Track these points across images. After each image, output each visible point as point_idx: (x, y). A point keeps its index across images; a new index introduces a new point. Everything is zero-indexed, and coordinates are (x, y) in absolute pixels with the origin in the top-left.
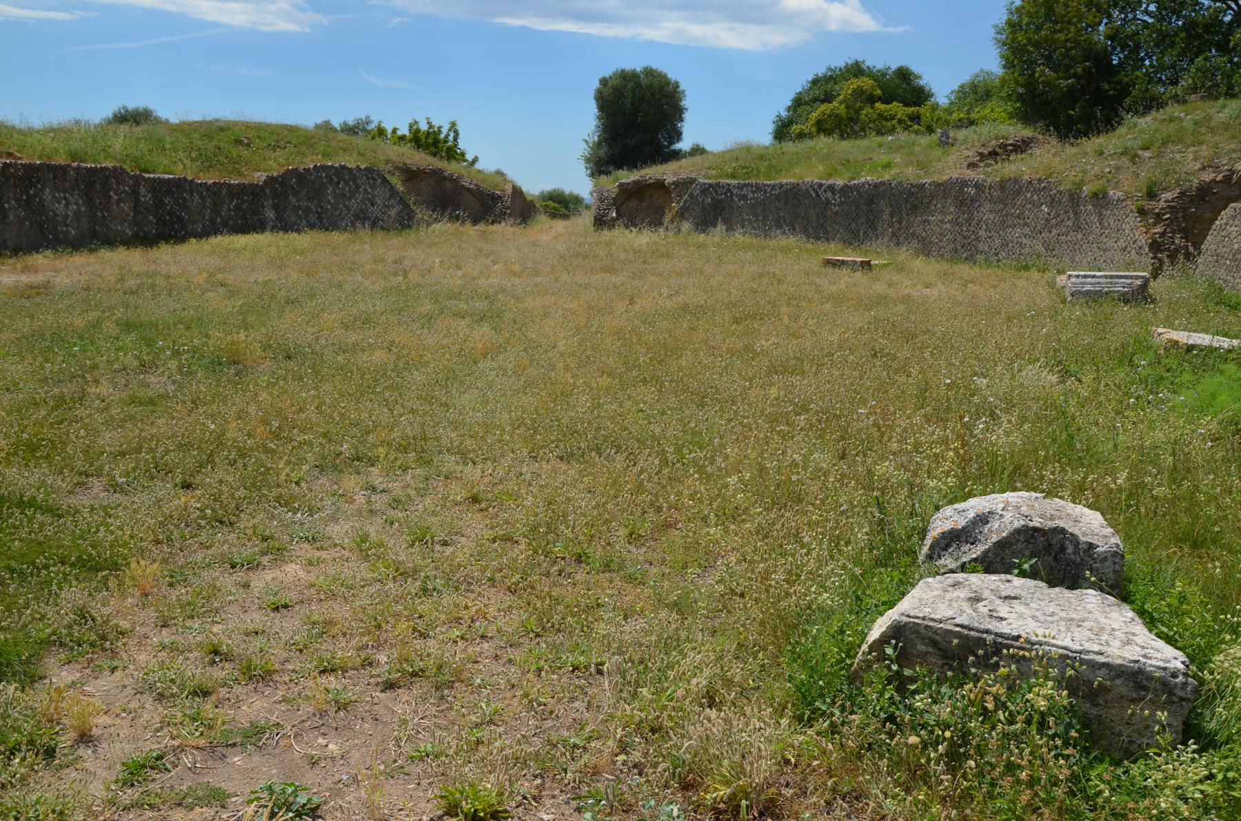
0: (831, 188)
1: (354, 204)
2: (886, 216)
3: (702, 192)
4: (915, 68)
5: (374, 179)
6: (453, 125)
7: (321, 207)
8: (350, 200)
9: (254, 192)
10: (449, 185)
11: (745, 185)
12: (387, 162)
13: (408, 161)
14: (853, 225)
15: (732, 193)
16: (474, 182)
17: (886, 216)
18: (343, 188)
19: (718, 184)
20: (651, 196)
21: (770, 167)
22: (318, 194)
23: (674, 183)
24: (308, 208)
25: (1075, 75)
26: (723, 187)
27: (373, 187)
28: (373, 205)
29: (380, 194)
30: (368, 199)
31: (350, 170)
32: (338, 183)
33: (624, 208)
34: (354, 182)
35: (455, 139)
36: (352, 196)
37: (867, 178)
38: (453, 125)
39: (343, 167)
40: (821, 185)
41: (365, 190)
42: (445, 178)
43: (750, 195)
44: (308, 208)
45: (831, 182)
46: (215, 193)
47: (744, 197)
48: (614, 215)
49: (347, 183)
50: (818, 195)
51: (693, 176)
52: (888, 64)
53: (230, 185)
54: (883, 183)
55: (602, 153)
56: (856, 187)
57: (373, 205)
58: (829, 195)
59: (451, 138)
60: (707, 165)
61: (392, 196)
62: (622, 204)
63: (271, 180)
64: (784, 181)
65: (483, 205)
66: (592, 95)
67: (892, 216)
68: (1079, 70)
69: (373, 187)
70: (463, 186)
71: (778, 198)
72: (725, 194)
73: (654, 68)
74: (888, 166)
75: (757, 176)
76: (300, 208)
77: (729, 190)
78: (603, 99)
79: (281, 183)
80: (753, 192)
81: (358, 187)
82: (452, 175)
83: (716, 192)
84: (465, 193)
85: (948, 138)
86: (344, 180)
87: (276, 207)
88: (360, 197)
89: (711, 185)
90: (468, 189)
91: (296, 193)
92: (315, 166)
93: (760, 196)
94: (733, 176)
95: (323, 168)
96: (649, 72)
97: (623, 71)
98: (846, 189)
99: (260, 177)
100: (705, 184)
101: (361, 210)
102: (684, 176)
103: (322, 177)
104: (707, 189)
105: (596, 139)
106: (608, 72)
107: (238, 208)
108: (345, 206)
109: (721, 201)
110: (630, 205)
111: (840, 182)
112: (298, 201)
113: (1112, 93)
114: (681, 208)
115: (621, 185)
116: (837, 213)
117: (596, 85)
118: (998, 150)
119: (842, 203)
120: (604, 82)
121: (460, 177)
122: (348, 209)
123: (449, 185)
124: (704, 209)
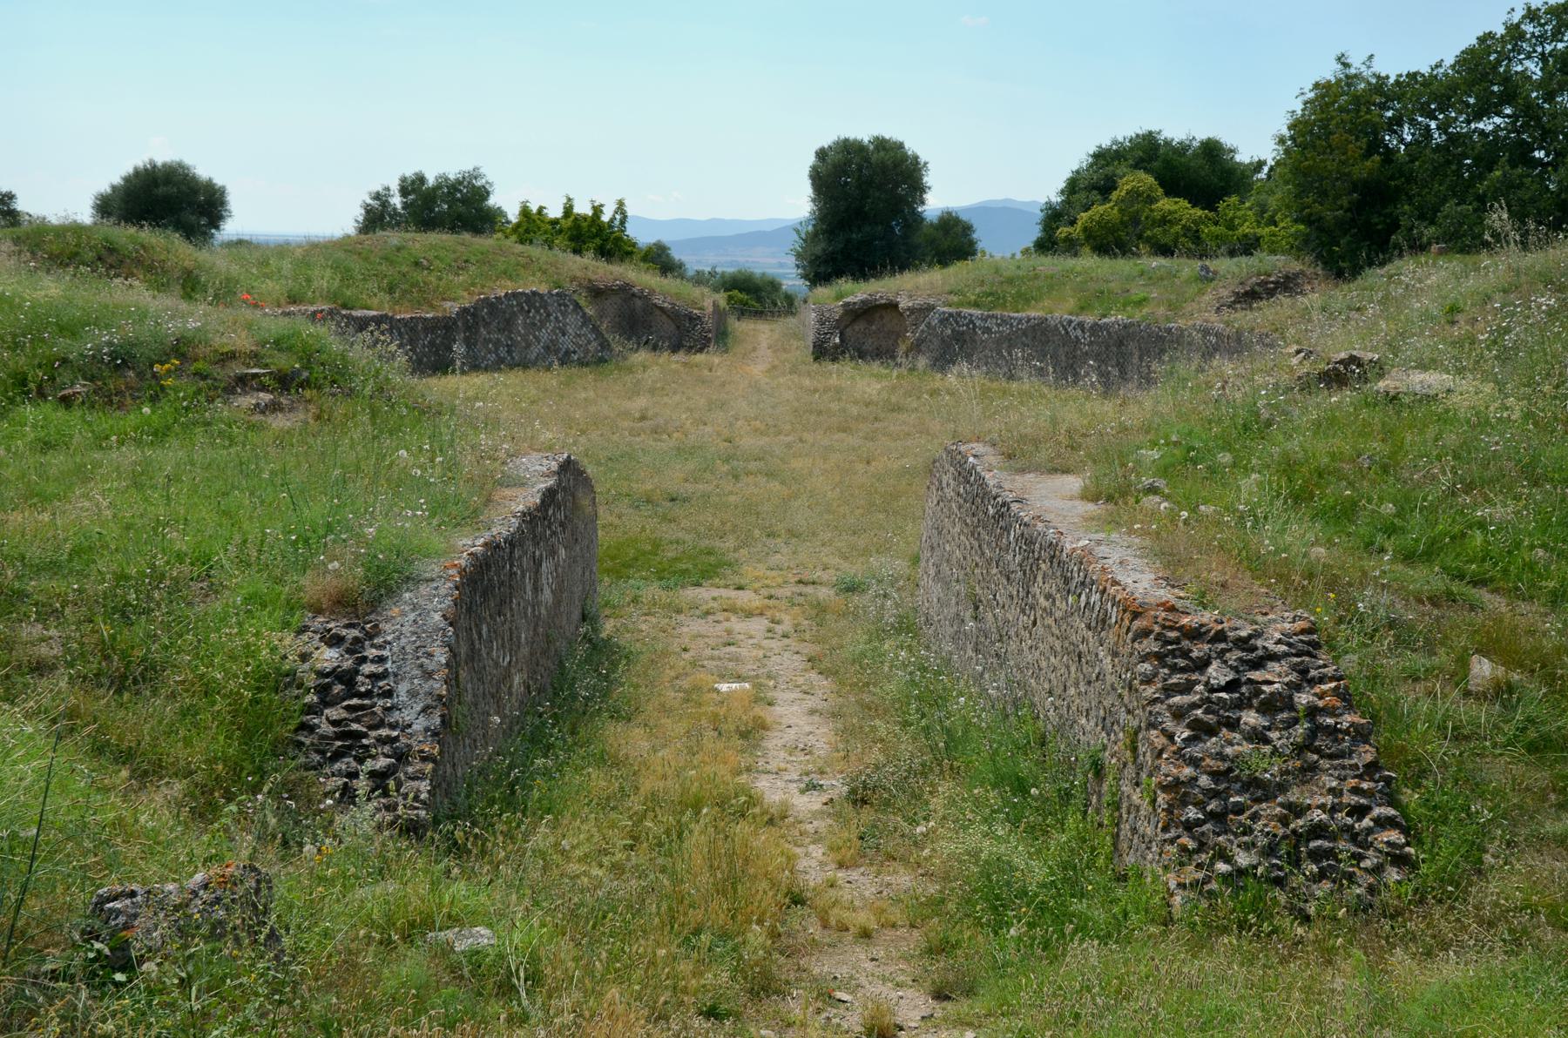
0: (1081, 325)
1: (544, 335)
2: (1135, 360)
3: (941, 321)
4: (1227, 140)
5: (566, 306)
6: (621, 204)
7: (511, 339)
8: (540, 330)
9: (446, 326)
10: (639, 303)
11: (989, 316)
12: (573, 279)
13: (593, 277)
14: (1103, 367)
15: (974, 325)
16: (668, 299)
17: (1135, 360)
18: (534, 317)
19: (959, 314)
20: (882, 318)
21: (1019, 295)
22: (508, 325)
23: (909, 309)
24: (498, 339)
25: (1341, 207)
26: (965, 318)
27: (564, 314)
28: (564, 335)
29: (573, 322)
30: (559, 328)
31: (541, 296)
32: (529, 311)
33: (849, 331)
34: (545, 309)
35: (623, 222)
36: (543, 323)
37: (1117, 317)
38: (621, 204)
39: (534, 293)
40: (1070, 322)
41: (556, 318)
42: (634, 295)
43: (995, 328)
44: (498, 339)
45: (1081, 318)
46: (412, 329)
47: (988, 330)
48: (837, 340)
49: (537, 311)
50: (1067, 333)
51: (931, 301)
52: (1193, 133)
53: (426, 319)
54: (1132, 324)
55: (818, 250)
56: (1106, 327)
57: (564, 335)
58: (1079, 332)
59: (617, 223)
60: (947, 288)
61: (584, 324)
62: (846, 327)
63: (464, 311)
64: (1033, 314)
65: (678, 327)
66: (806, 171)
67: (1141, 359)
68: (1345, 204)
69: (564, 314)
70: (655, 305)
71: (1025, 333)
72: (967, 325)
73: (887, 137)
74: (1140, 303)
75: (1004, 307)
76: (490, 340)
77: (971, 321)
78: (820, 178)
79: (473, 315)
80: (998, 325)
81: (549, 315)
82: (642, 291)
83: (957, 323)
84: (658, 312)
85: (1208, 272)
86: (535, 308)
87: (469, 343)
88: (550, 326)
89: (951, 315)
90: (662, 309)
91: (487, 325)
92: (507, 294)
93: (1005, 329)
94: (976, 305)
95: (515, 295)
96: (881, 144)
97: (846, 140)
98: (1095, 328)
99: (452, 308)
100: (944, 313)
101: (552, 341)
102: (919, 301)
103: (512, 306)
104: (947, 319)
105: (810, 228)
106: (826, 141)
107: (432, 343)
108: (535, 337)
109: (963, 333)
110: (857, 328)
111: (1089, 319)
112: (489, 333)
113: (1380, 227)
114: (918, 340)
115: (847, 304)
116: (1086, 353)
117: (811, 159)
118: (1257, 288)
119: (1091, 343)
120: (822, 154)
121: (652, 292)
122: (538, 340)
123: (639, 303)
124: (943, 341)
